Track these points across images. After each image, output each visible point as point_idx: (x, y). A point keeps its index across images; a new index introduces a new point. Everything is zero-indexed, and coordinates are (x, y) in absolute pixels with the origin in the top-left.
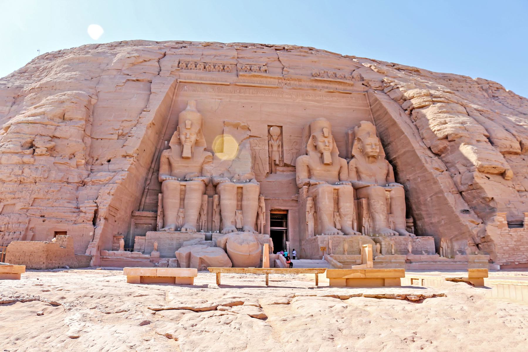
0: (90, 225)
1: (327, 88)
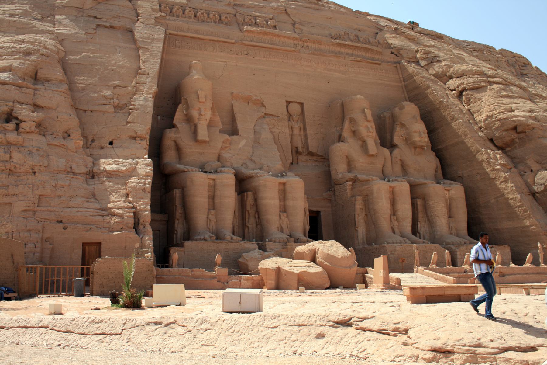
0: (132, 234)
1: (352, 55)
